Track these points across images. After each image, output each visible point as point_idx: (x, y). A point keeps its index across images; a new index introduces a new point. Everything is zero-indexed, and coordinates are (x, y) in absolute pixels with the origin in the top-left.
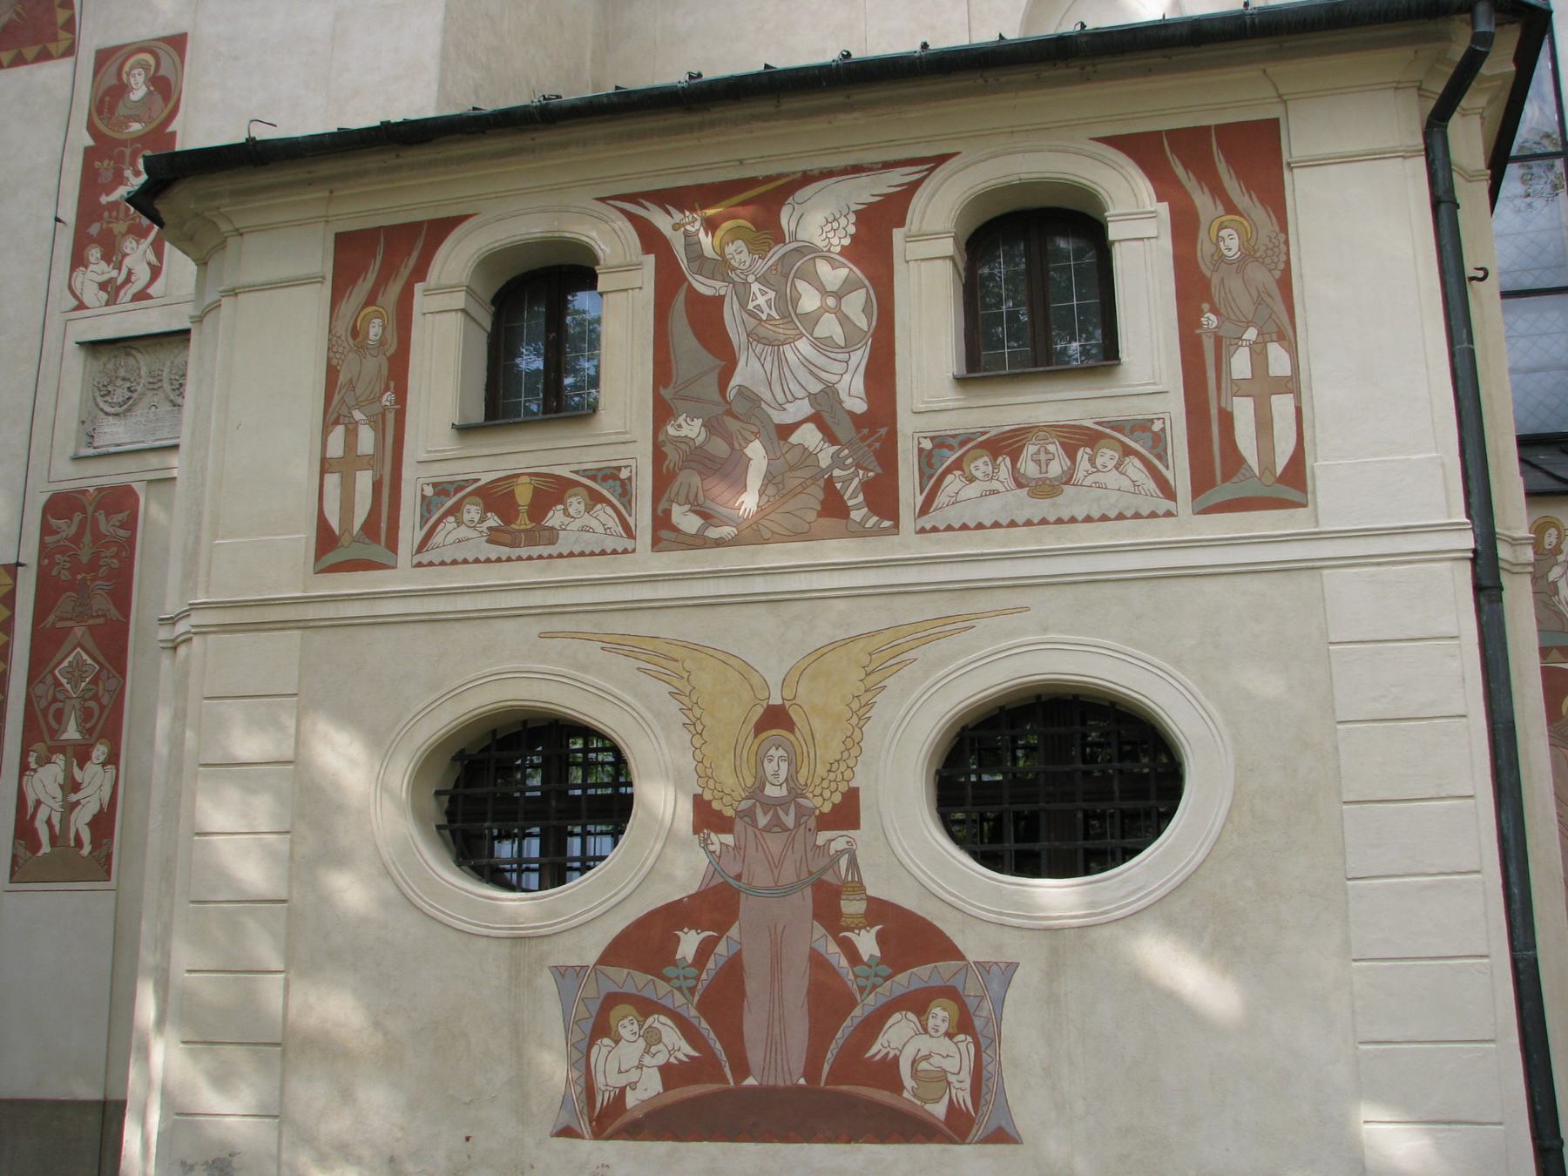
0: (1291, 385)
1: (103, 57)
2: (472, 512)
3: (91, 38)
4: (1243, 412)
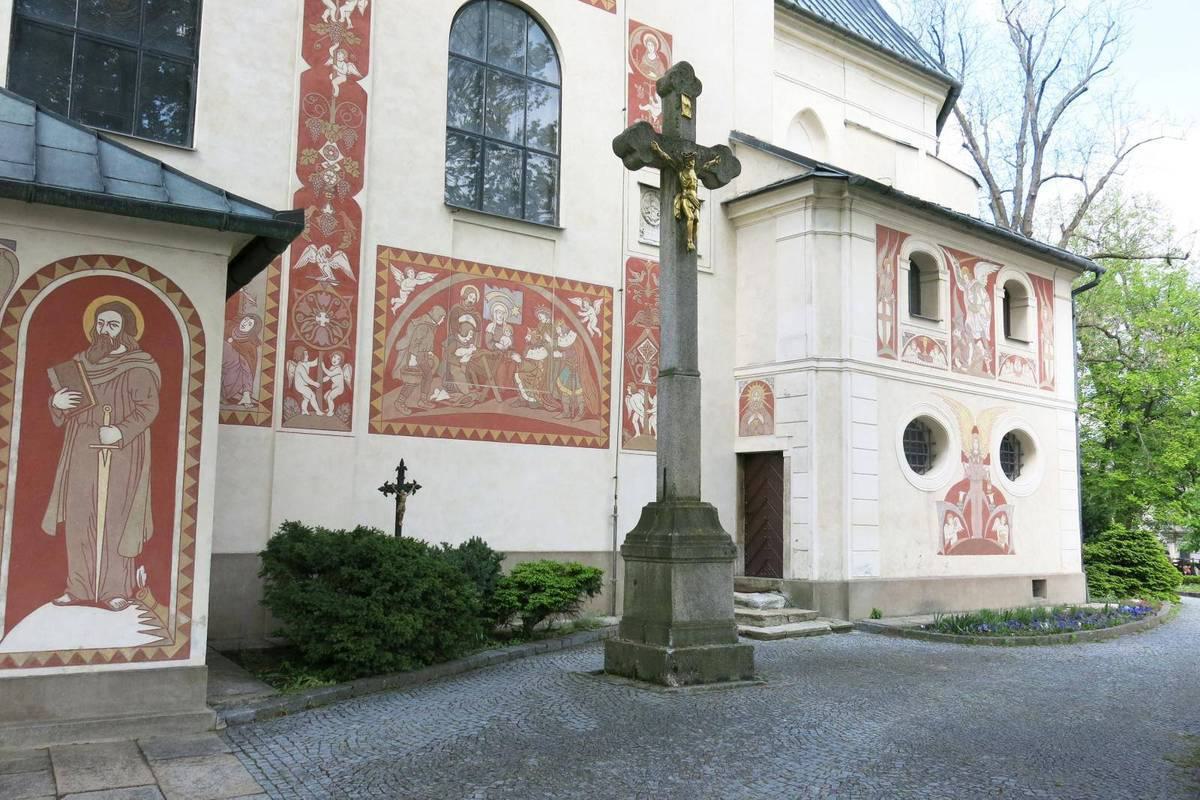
2: (914, 345)
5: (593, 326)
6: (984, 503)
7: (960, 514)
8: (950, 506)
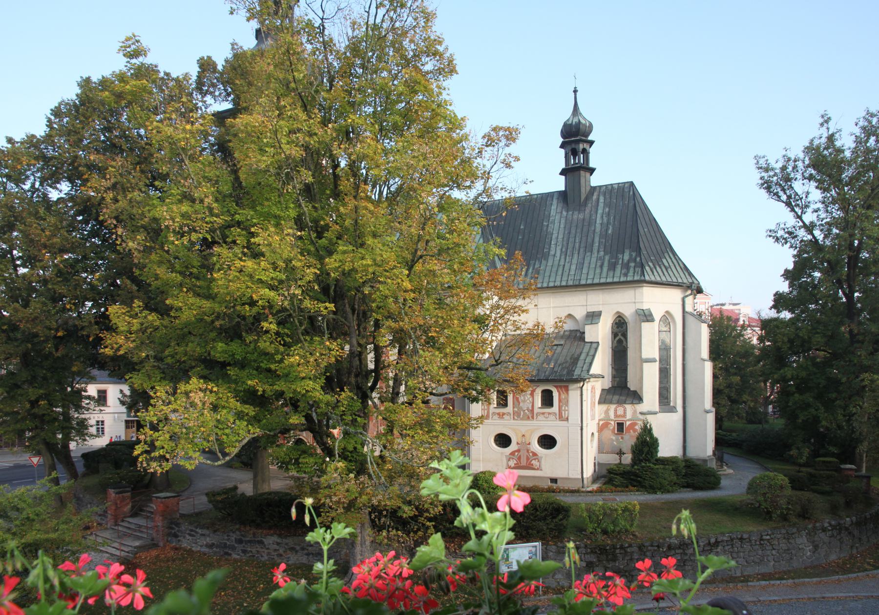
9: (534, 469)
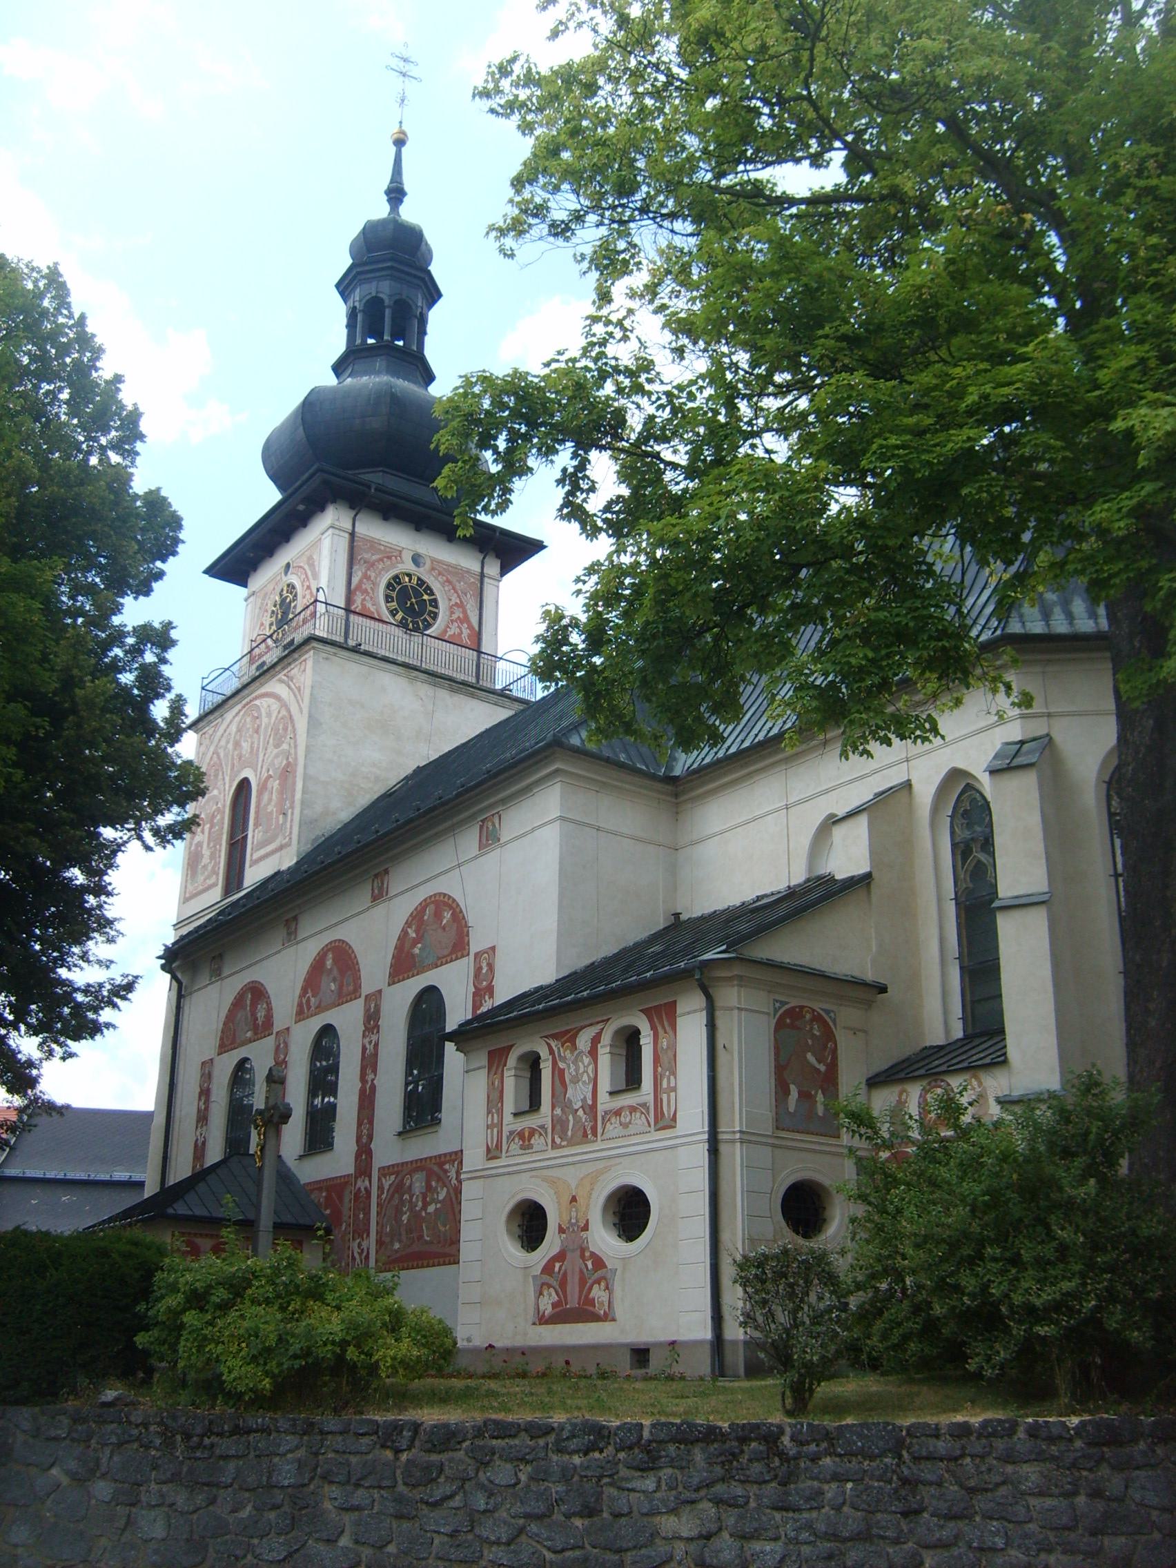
0: (674, 1089)
1: (477, 955)
2: (517, 1140)
3: (474, 948)
4: (665, 1097)
5: (454, 1181)
6: (581, 1271)
7: (555, 1283)
8: (546, 1278)
9: (595, 1318)
